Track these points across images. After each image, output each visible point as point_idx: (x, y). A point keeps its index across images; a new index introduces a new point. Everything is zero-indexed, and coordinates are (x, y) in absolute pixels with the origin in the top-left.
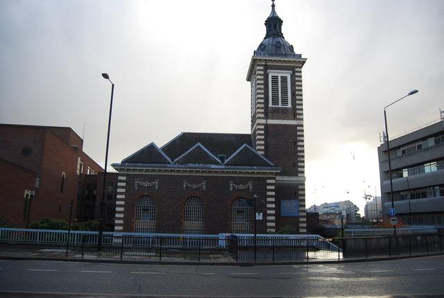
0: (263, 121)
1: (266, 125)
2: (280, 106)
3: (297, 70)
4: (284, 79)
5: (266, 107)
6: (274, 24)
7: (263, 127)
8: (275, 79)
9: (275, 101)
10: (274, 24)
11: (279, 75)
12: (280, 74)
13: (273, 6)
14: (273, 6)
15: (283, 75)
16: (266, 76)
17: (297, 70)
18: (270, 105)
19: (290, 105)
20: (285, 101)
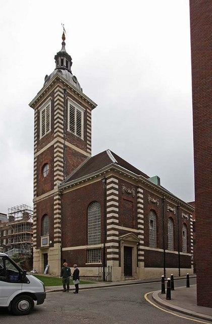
0: (62, 141)
1: (65, 146)
2: (75, 134)
3: (88, 110)
4: (79, 114)
5: (66, 133)
6: (63, 60)
7: (62, 146)
8: (72, 109)
9: (72, 129)
10: (63, 60)
11: (76, 108)
12: (77, 108)
13: (64, 44)
14: (64, 44)
15: (78, 109)
16: (66, 103)
17: (88, 110)
18: (68, 130)
19: (82, 138)
20: (79, 133)
